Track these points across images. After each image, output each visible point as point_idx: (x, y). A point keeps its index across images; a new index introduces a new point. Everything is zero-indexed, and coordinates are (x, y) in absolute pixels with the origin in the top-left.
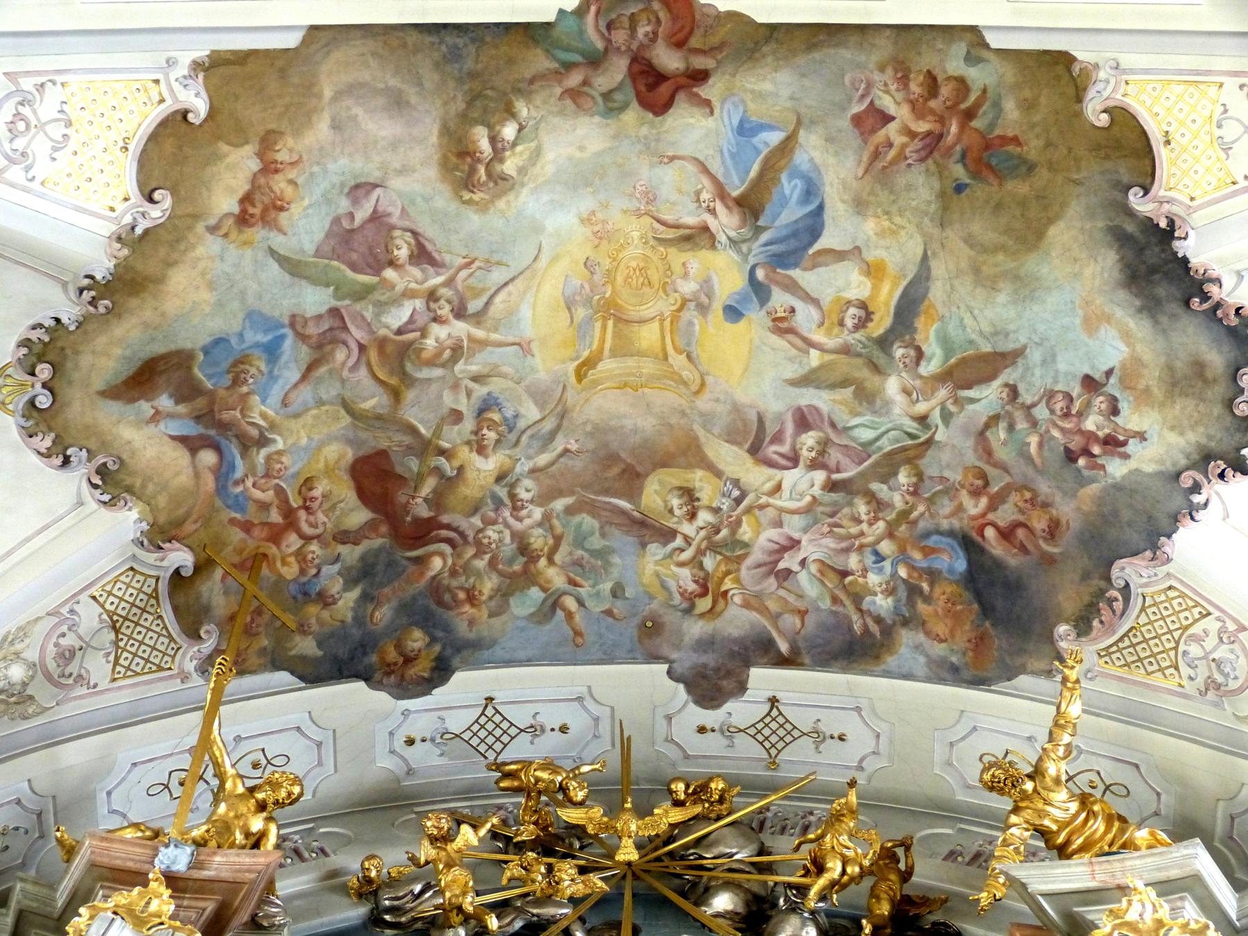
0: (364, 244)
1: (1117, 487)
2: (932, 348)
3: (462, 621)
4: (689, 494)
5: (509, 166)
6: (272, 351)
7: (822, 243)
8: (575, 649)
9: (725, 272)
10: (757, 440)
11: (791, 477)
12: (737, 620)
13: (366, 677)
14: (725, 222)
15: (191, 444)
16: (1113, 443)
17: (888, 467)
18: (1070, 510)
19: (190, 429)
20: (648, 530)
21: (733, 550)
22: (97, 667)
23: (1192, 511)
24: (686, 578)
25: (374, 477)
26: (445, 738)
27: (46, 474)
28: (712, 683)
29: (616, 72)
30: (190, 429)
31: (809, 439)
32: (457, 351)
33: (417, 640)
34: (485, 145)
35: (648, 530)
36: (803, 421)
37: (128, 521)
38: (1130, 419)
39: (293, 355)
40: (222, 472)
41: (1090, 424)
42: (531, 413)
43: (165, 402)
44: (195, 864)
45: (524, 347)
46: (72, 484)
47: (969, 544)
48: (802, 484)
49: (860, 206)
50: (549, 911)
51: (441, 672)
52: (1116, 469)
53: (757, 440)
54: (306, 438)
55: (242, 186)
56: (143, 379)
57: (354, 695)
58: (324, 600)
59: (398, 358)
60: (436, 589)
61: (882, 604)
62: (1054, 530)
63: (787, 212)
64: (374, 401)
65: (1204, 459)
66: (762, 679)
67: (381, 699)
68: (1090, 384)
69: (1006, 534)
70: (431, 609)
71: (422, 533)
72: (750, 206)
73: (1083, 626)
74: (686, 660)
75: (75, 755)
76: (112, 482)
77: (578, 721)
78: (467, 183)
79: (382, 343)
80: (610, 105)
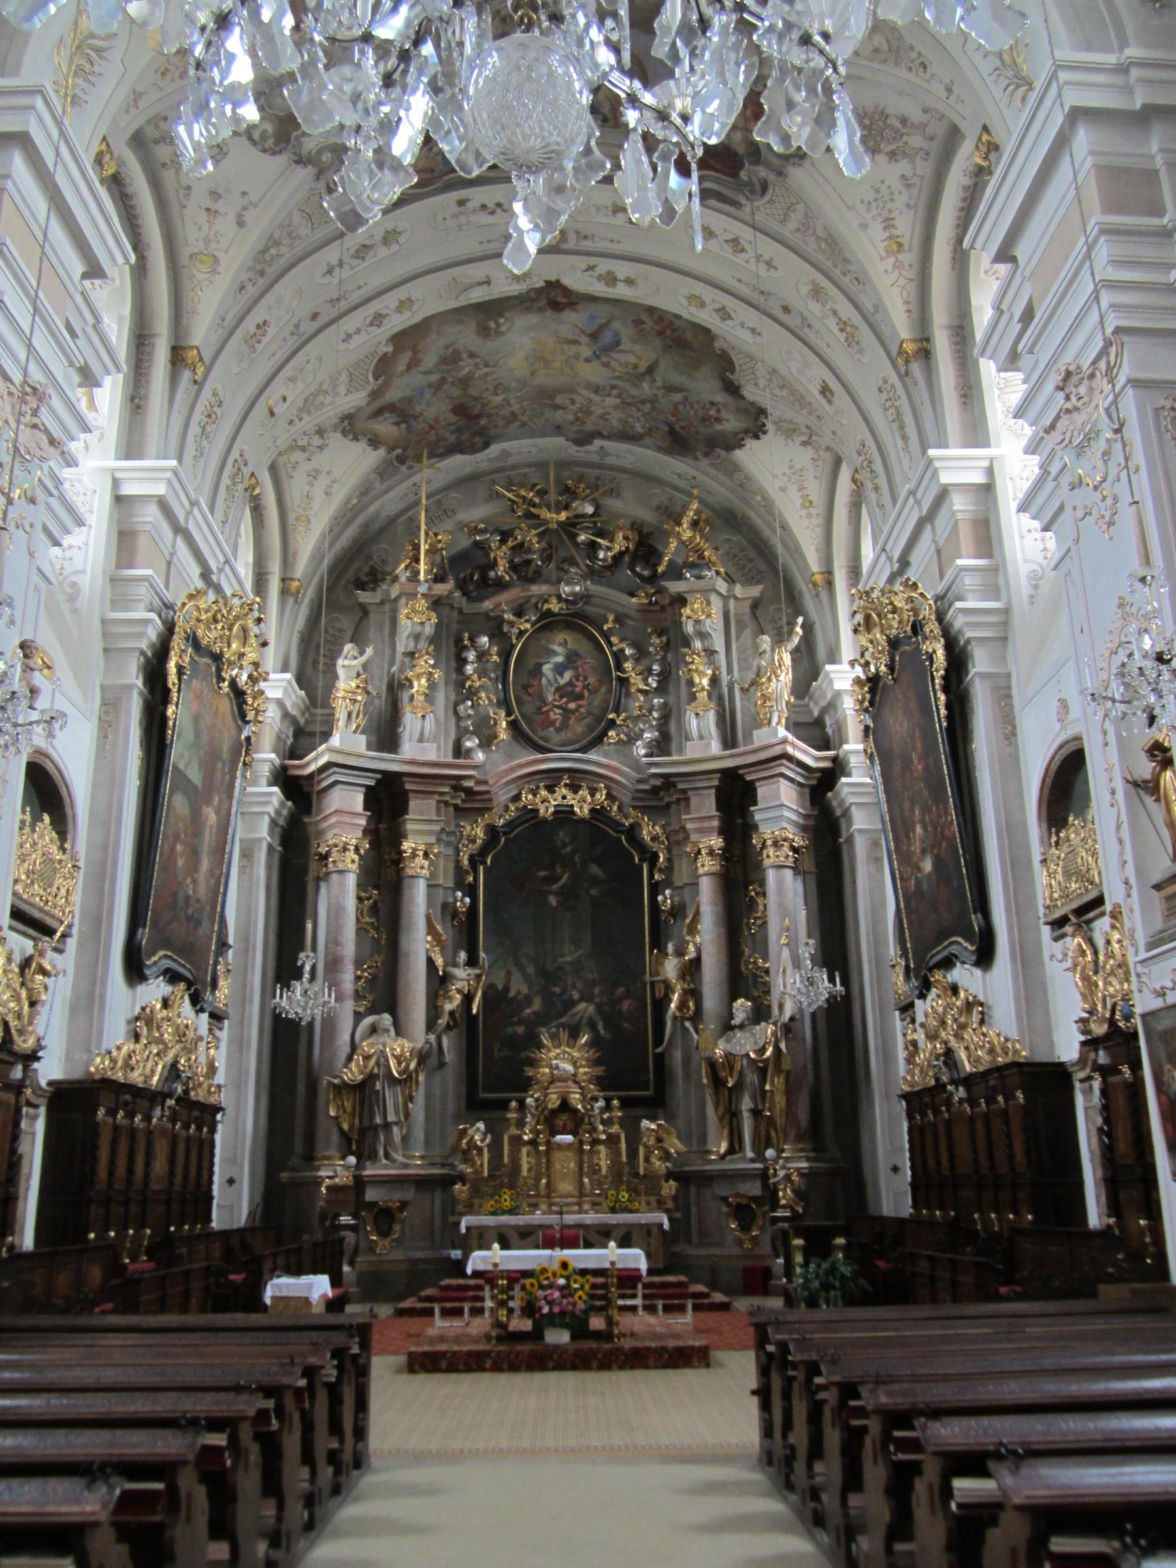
0: (452, 358)
1: (718, 432)
2: (659, 379)
3: (493, 432)
4: (573, 402)
5: (503, 329)
6: (421, 394)
7: (622, 347)
8: (533, 434)
9: (586, 351)
10: (597, 390)
11: (608, 399)
12: (589, 426)
13: (462, 452)
14: (584, 339)
15: (397, 424)
16: (718, 420)
17: (643, 402)
18: (705, 431)
19: (397, 419)
20: (557, 407)
21: (589, 413)
22: (377, 485)
23: (741, 446)
24: (572, 418)
25: (460, 410)
26: (490, 460)
27: (354, 443)
28: (583, 439)
29: (543, 302)
30: (397, 419)
31: (615, 392)
32: (486, 375)
33: (477, 439)
34: (493, 325)
35: (557, 407)
36: (613, 387)
37: (381, 452)
38: (724, 415)
39: (428, 395)
40: (409, 429)
41: (712, 412)
42: (514, 384)
43: (387, 415)
44: (430, 589)
45: (511, 370)
46: (362, 445)
47: (669, 425)
48: (611, 401)
49: (634, 342)
50: (530, 557)
51: (486, 445)
52: (718, 427)
53: (597, 390)
54: (436, 409)
55: (407, 360)
56: (379, 412)
57: (458, 459)
58: (445, 440)
59: (465, 382)
60: (483, 428)
61: (640, 430)
62: (697, 433)
63: (607, 337)
64: (456, 392)
65: (746, 432)
66: (598, 443)
67: (466, 458)
68: (712, 403)
69: (683, 428)
70: (482, 432)
71: (478, 416)
72: (594, 336)
73: (706, 455)
74: (572, 436)
75: (372, 509)
76: (374, 443)
77: (534, 450)
78: (488, 335)
79: (460, 380)
80: (540, 310)
